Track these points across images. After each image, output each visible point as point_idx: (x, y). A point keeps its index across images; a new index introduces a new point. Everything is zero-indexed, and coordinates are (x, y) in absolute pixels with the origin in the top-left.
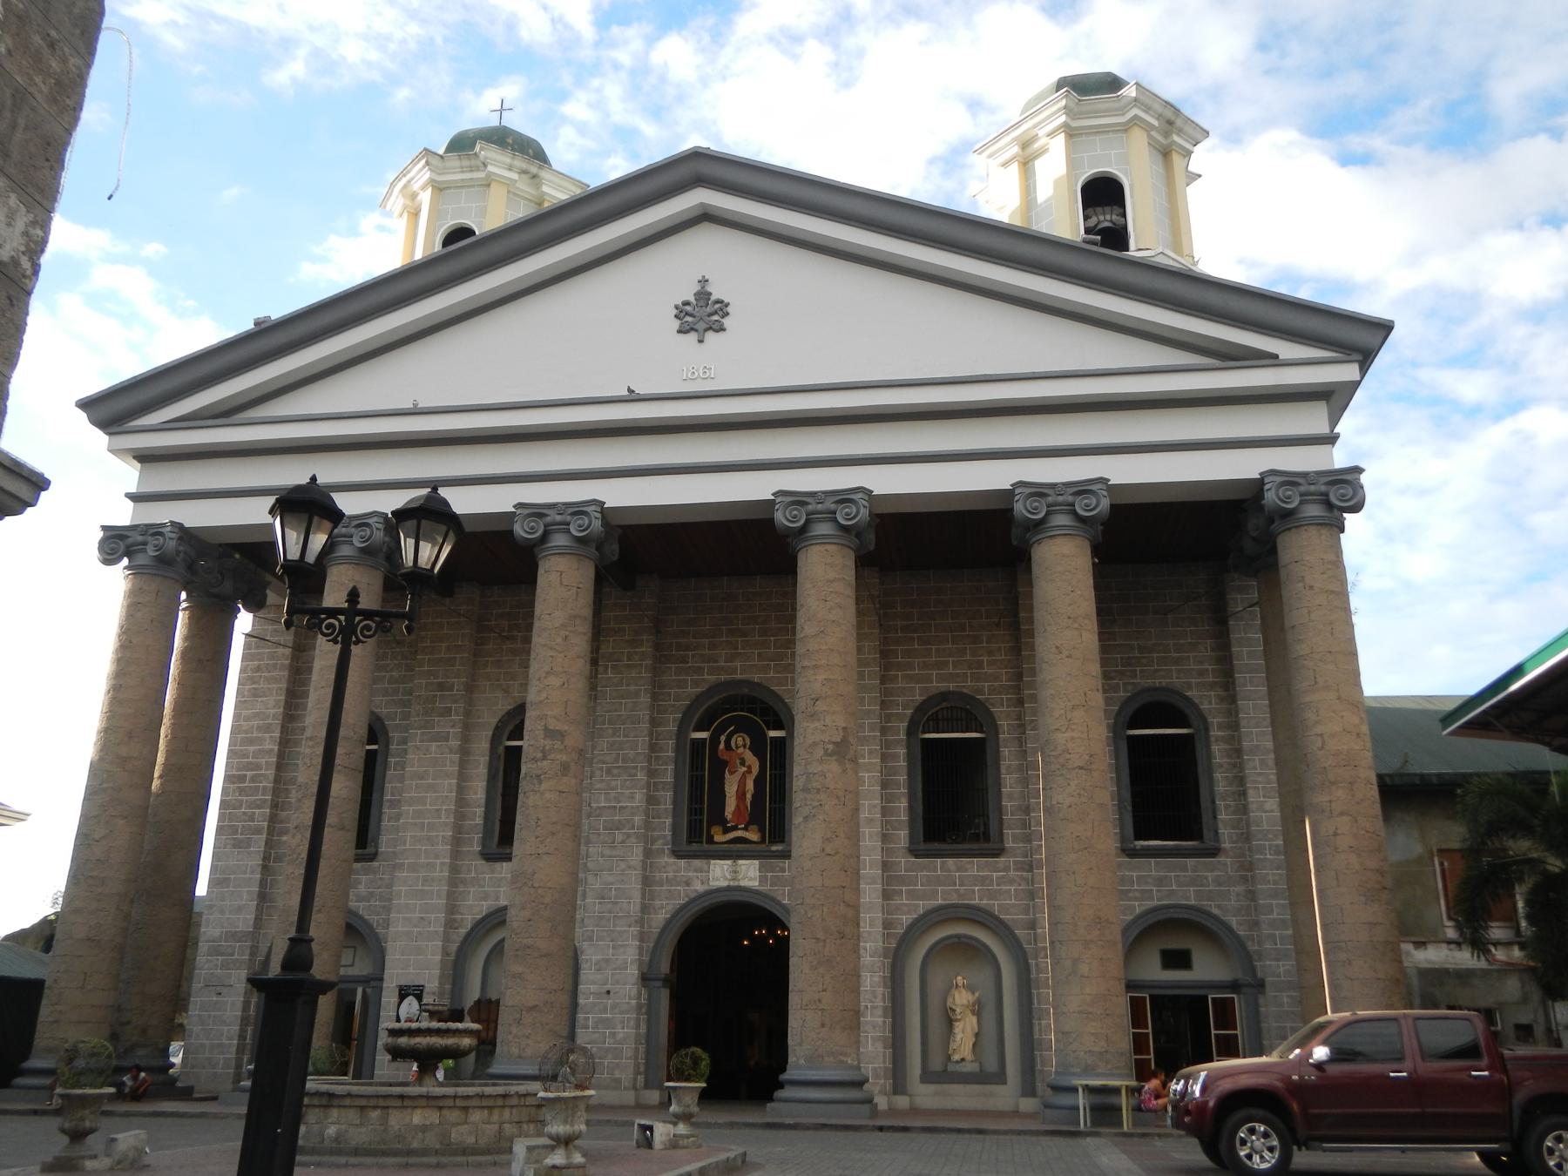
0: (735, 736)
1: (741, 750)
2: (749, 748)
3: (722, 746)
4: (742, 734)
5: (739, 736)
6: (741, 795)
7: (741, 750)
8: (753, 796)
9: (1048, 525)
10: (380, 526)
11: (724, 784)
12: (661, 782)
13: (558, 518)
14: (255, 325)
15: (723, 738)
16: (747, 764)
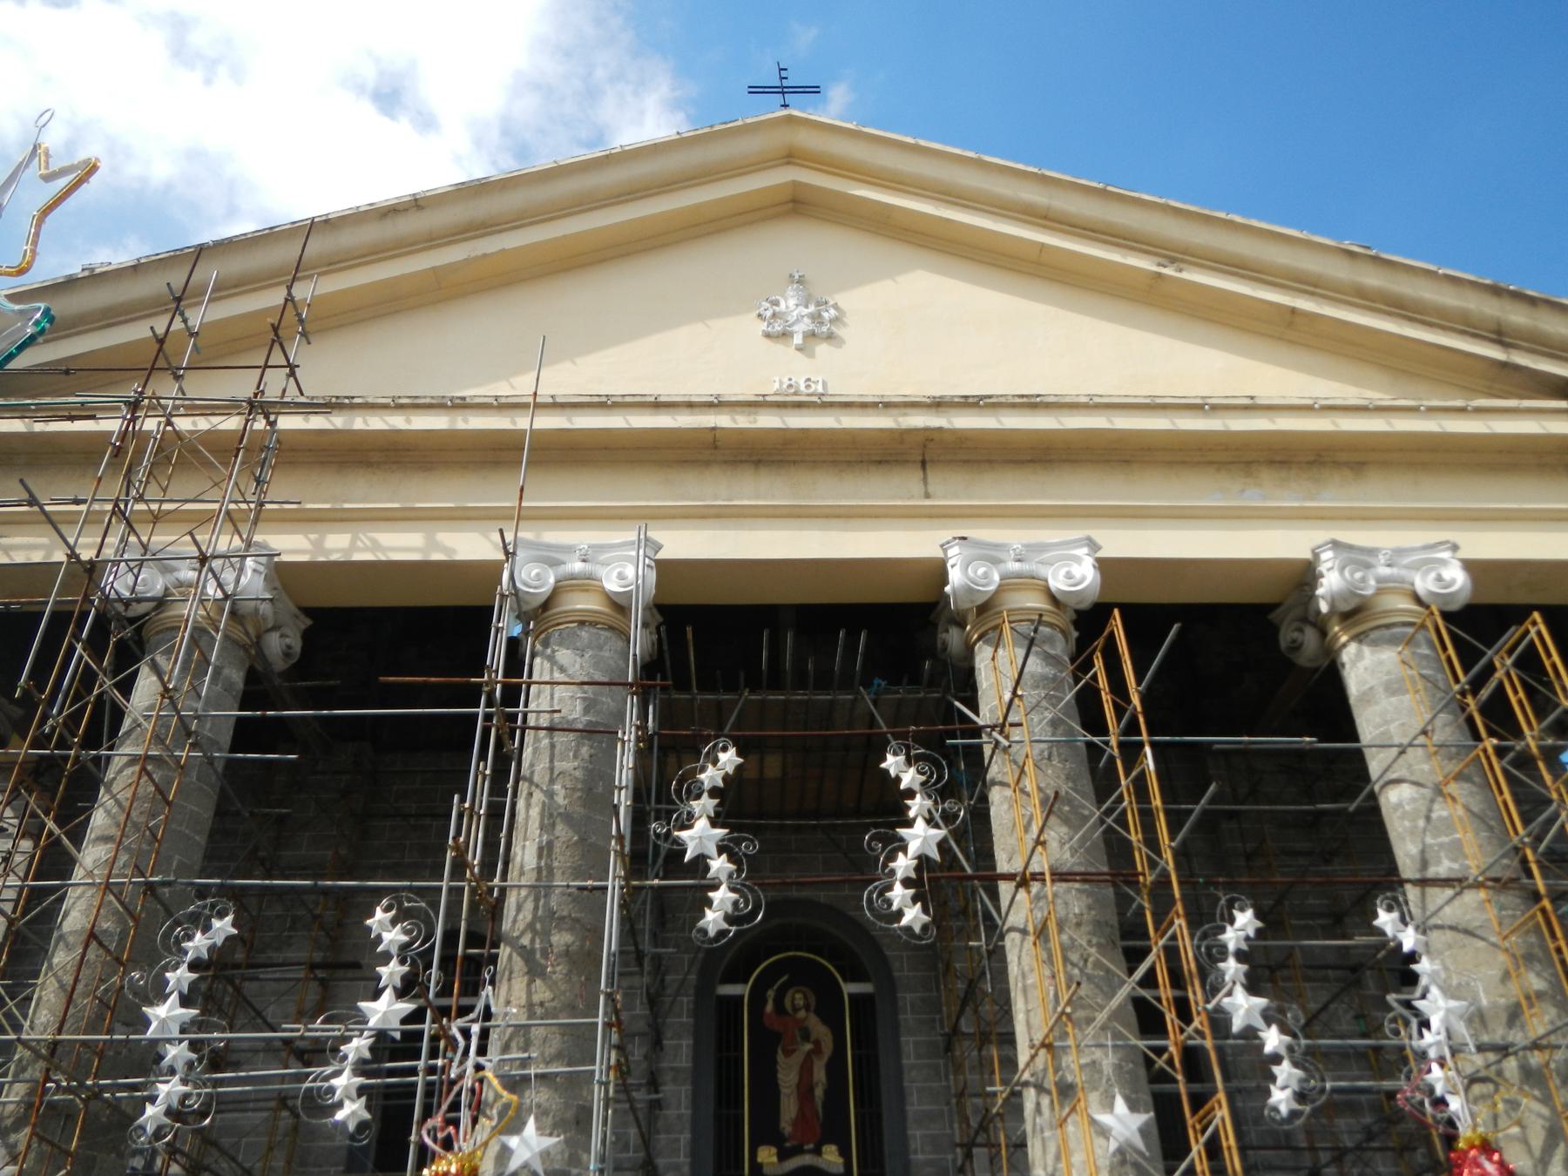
0: (790, 992)
1: (802, 1014)
2: (818, 1012)
3: (769, 1007)
4: (803, 988)
5: (798, 991)
6: (805, 1090)
7: (802, 1014)
8: (827, 1093)
9: (1368, 613)
10: (261, 568)
11: (776, 1072)
12: (672, 1069)
13: (577, 566)
14: (83, 270)
15: (771, 994)
16: (812, 1039)
